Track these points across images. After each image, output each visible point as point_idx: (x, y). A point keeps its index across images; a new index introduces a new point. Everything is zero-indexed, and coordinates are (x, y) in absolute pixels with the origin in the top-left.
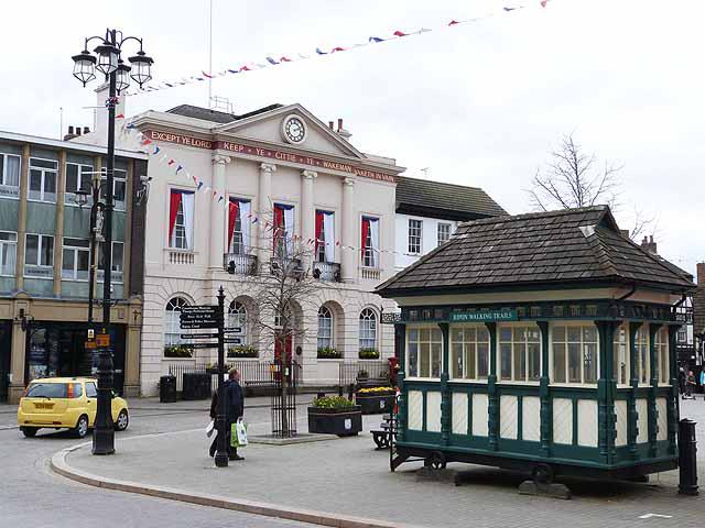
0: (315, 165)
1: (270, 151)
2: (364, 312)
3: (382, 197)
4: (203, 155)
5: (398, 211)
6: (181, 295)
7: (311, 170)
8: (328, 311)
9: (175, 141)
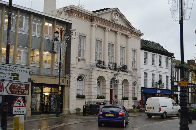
3: (135, 44)
4: (87, 23)
5: (142, 49)
6: (82, 75)
8: (125, 81)
9: (80, 17)
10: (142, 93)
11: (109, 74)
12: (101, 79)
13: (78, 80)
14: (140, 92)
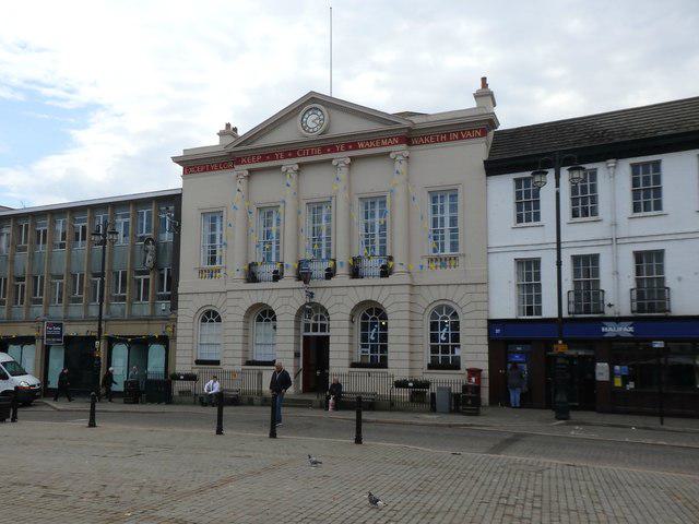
0: (347, 149)
1: (290, 151)
2: (439, 309)
7: (342, 157)
10: (493, 342)
11: (290, 293)
12: (264, 314)
13: (204, 320)
14: (486, 338)
